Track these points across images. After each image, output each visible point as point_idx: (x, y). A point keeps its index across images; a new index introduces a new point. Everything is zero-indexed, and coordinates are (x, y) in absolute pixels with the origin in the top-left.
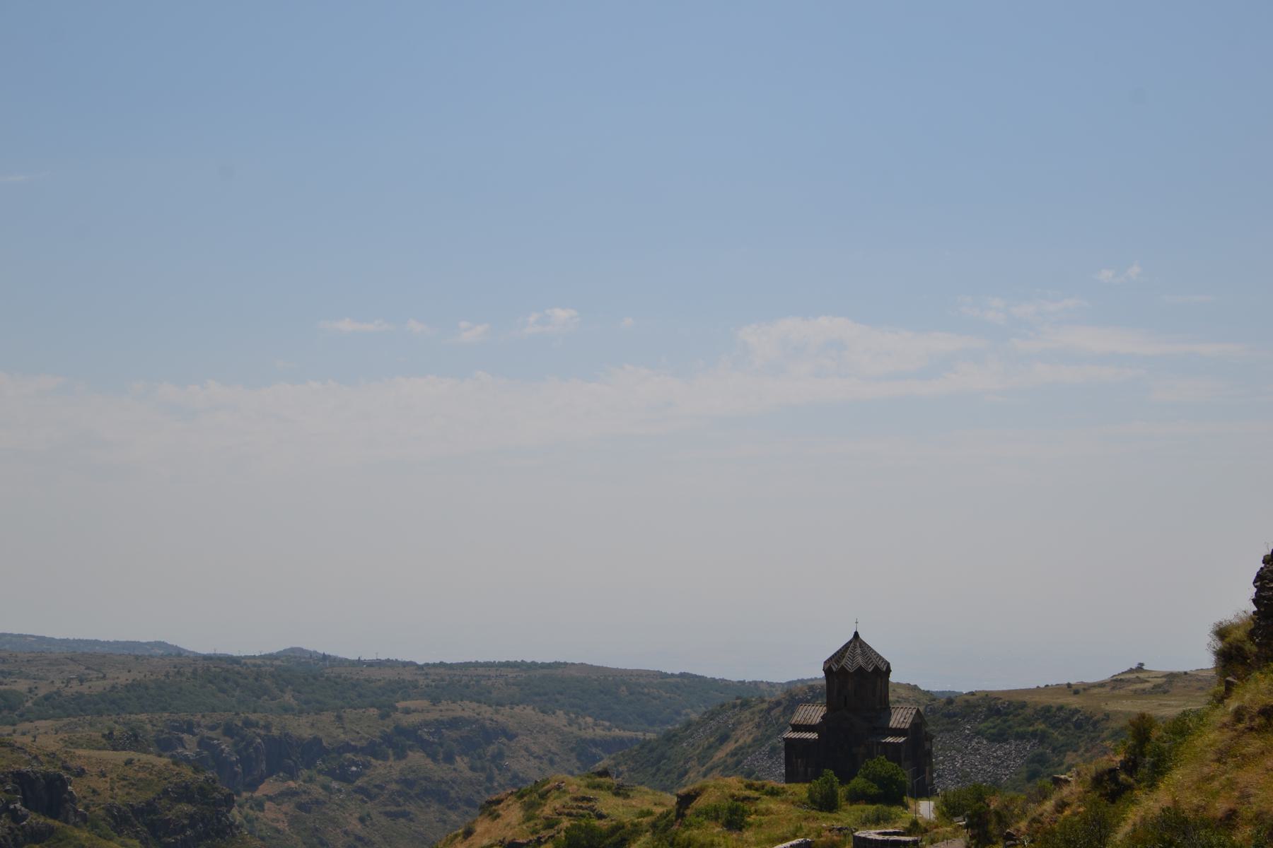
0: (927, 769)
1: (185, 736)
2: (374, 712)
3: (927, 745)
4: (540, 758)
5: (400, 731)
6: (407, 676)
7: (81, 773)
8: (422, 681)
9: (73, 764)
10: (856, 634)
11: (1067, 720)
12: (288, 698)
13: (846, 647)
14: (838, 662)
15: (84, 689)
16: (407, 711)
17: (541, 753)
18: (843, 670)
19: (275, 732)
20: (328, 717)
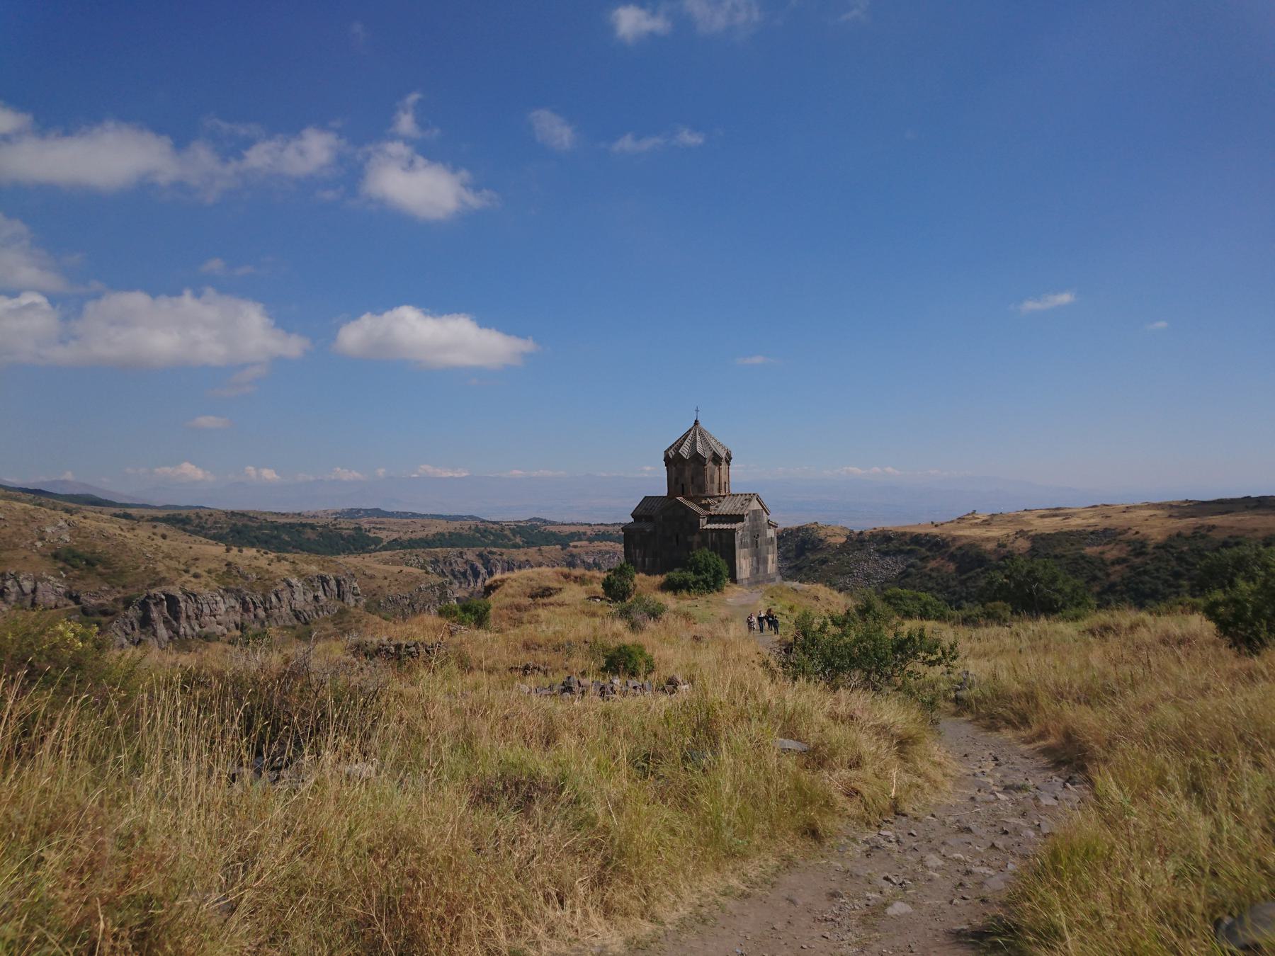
0: (770, 557)
1: (459, 560)
2: (558, 547)
5: (572, 556)
6: (582, 529)
7: (372, 577)
8: (589, 532)
9: (368, 572)
10: (696, 422)
11: (929, 541)
12: (518, 540)
13: (686, 436)
15: (413, 536)
16: (575, 547)
18: (678, 455)
19: (505, 557)
20: (533, 550)
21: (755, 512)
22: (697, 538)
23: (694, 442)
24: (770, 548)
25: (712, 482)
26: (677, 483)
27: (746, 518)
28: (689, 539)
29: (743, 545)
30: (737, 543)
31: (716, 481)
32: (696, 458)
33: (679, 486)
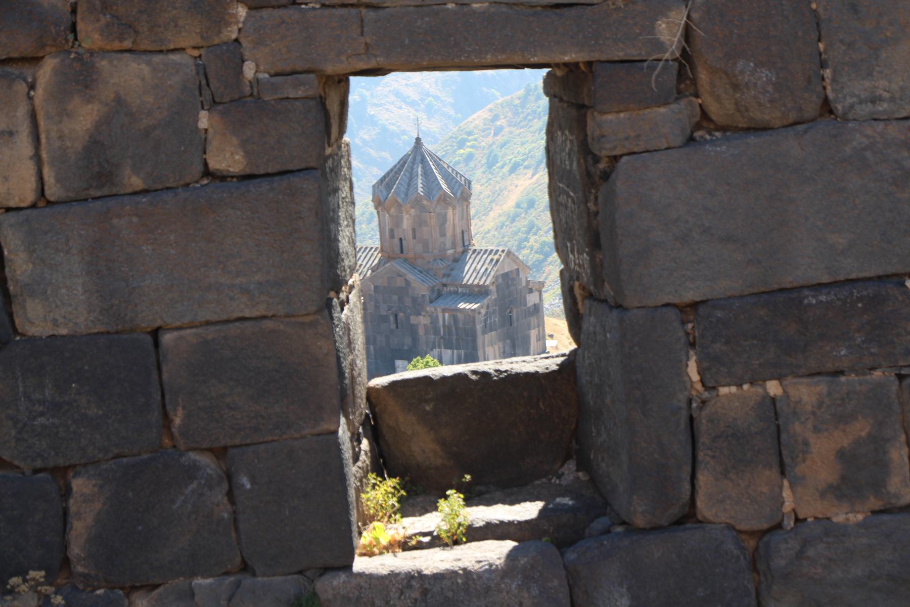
0: (533, 333)
3: (532, 299)
4: (412, 104)
10: (418, 140)
13: (403, 162)
14: (389, 187)
17: (415, 97)
21: (506, 276)
22: (422, 320)
23: (412, 178)
24: (533, 320)
25: (443, 234)
26: (392, 236)
27: (493, 288)
28: (413, 320)
29: (488, 328)
30: (479, 327)
31: (449, 233)
32: (417, 202)
33: (396, 241)
